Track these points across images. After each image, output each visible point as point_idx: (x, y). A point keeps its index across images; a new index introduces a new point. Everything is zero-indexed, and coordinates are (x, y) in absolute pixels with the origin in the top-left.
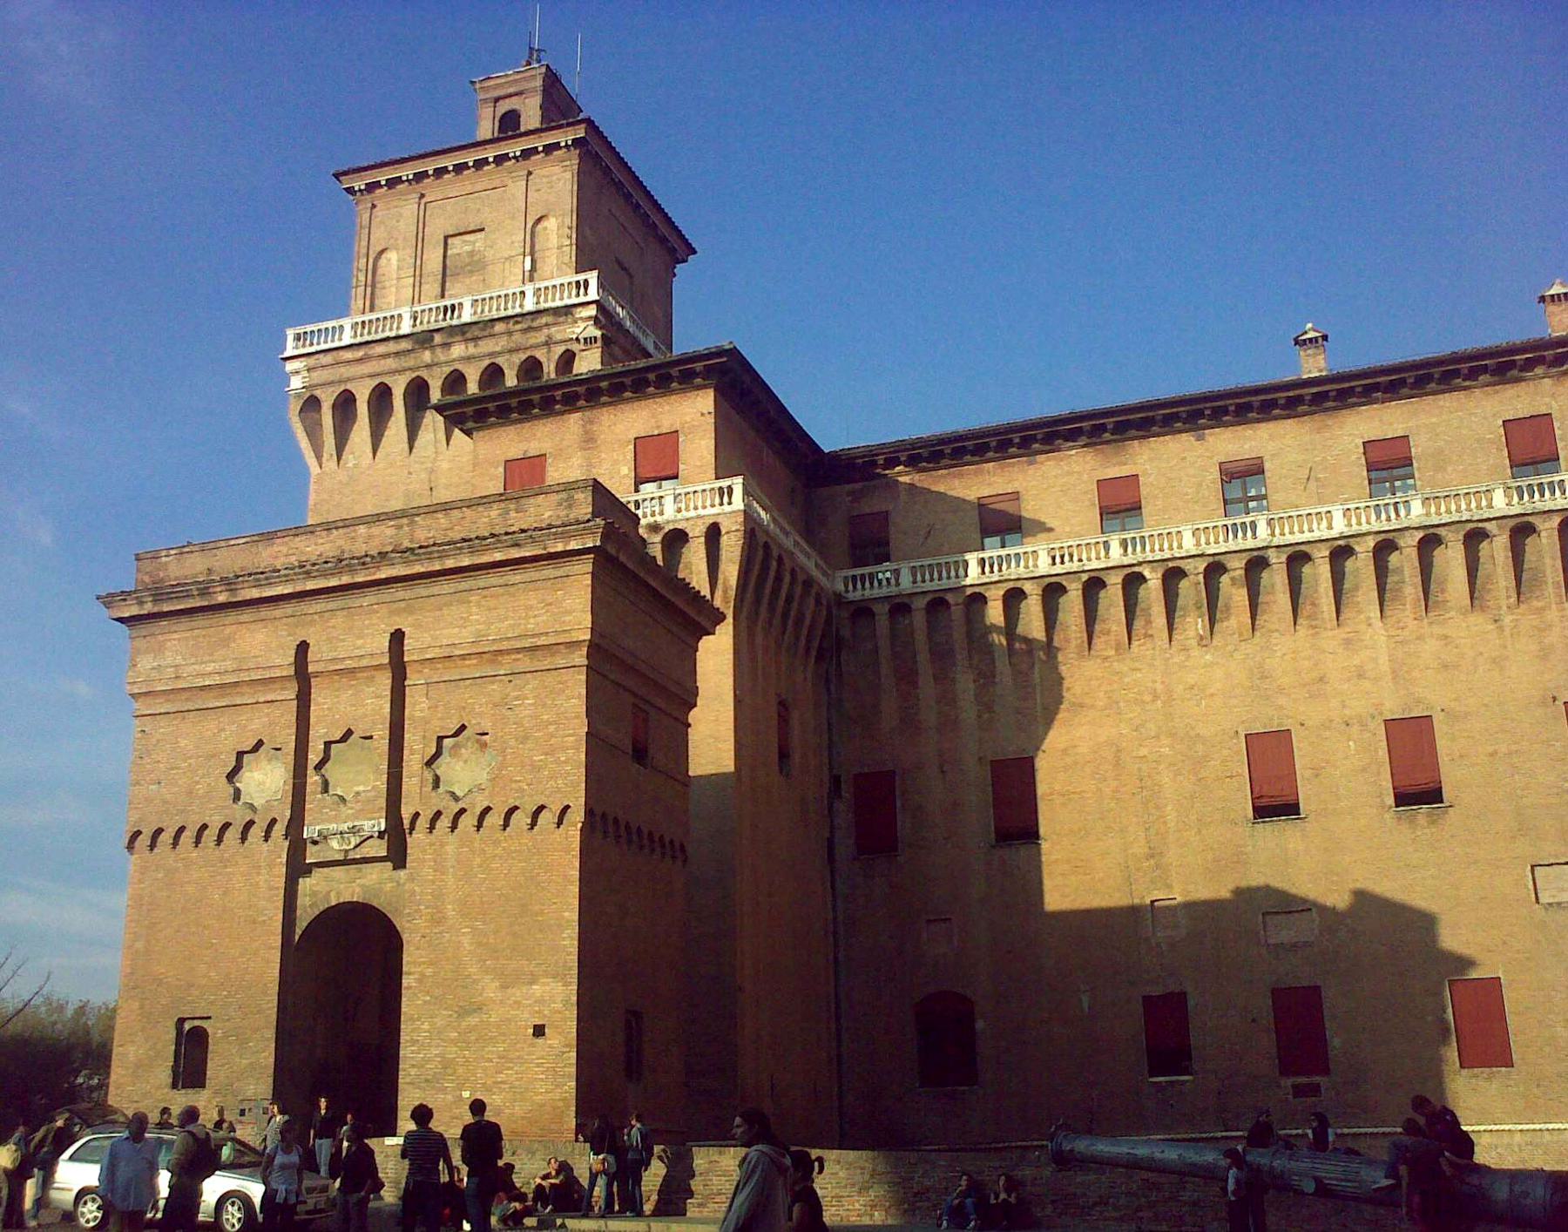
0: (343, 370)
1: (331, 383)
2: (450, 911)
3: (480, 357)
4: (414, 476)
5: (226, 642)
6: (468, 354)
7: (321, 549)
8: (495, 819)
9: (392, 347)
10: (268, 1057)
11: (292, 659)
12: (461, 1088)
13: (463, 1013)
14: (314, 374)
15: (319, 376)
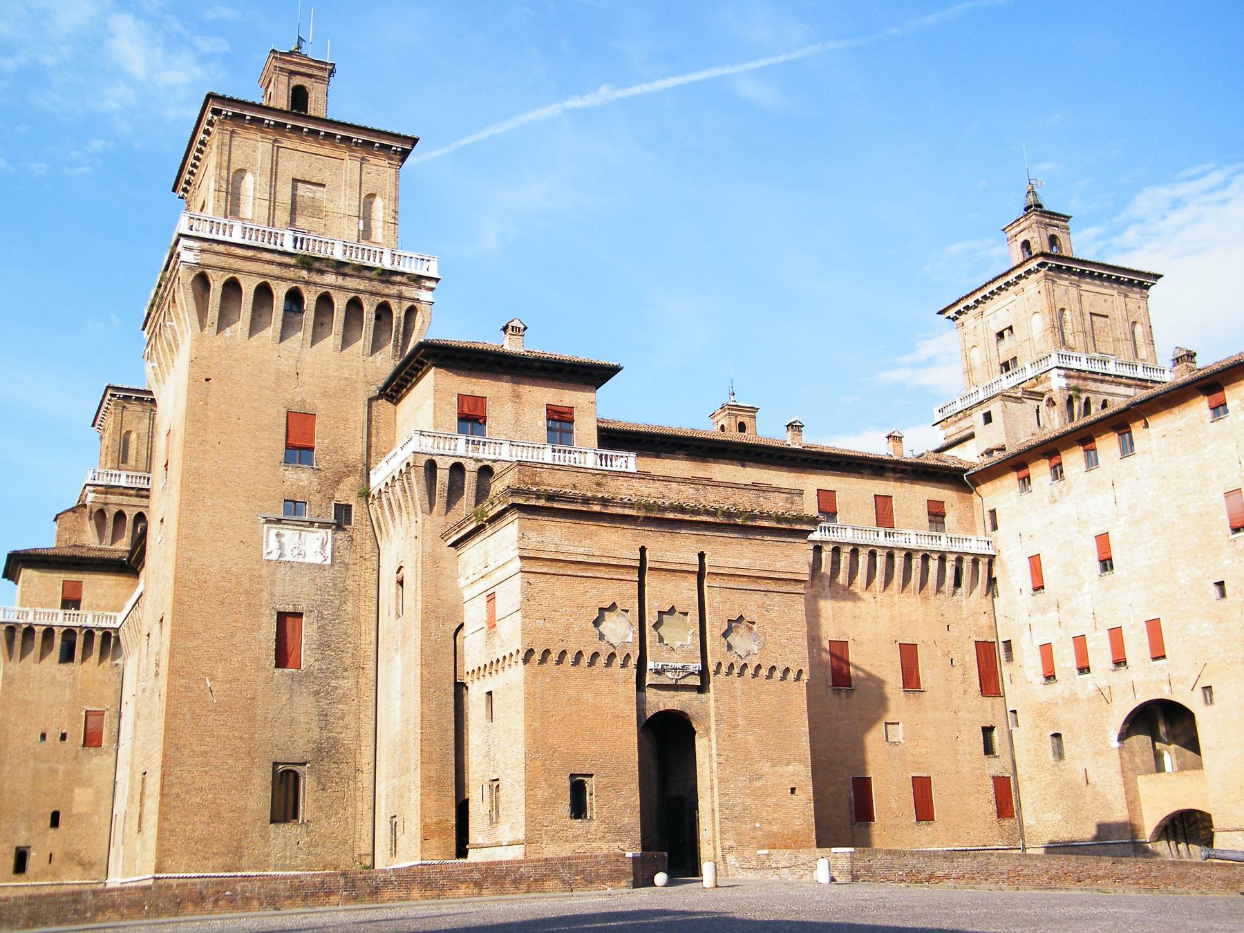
0: (231, 260)
1: (223, 269)
2: (740, 721)
3: (348, 290)
4: (282, 360)
5: (590, 535)
6: (337, 284)
7: (651, 490)
8: (764, 672)
9: (278, 258)
10: (636, 800)
11: (639, 557)
12: (754, 821)
13: (751, 779)
14: (204, 255)
15: (208, 259)
